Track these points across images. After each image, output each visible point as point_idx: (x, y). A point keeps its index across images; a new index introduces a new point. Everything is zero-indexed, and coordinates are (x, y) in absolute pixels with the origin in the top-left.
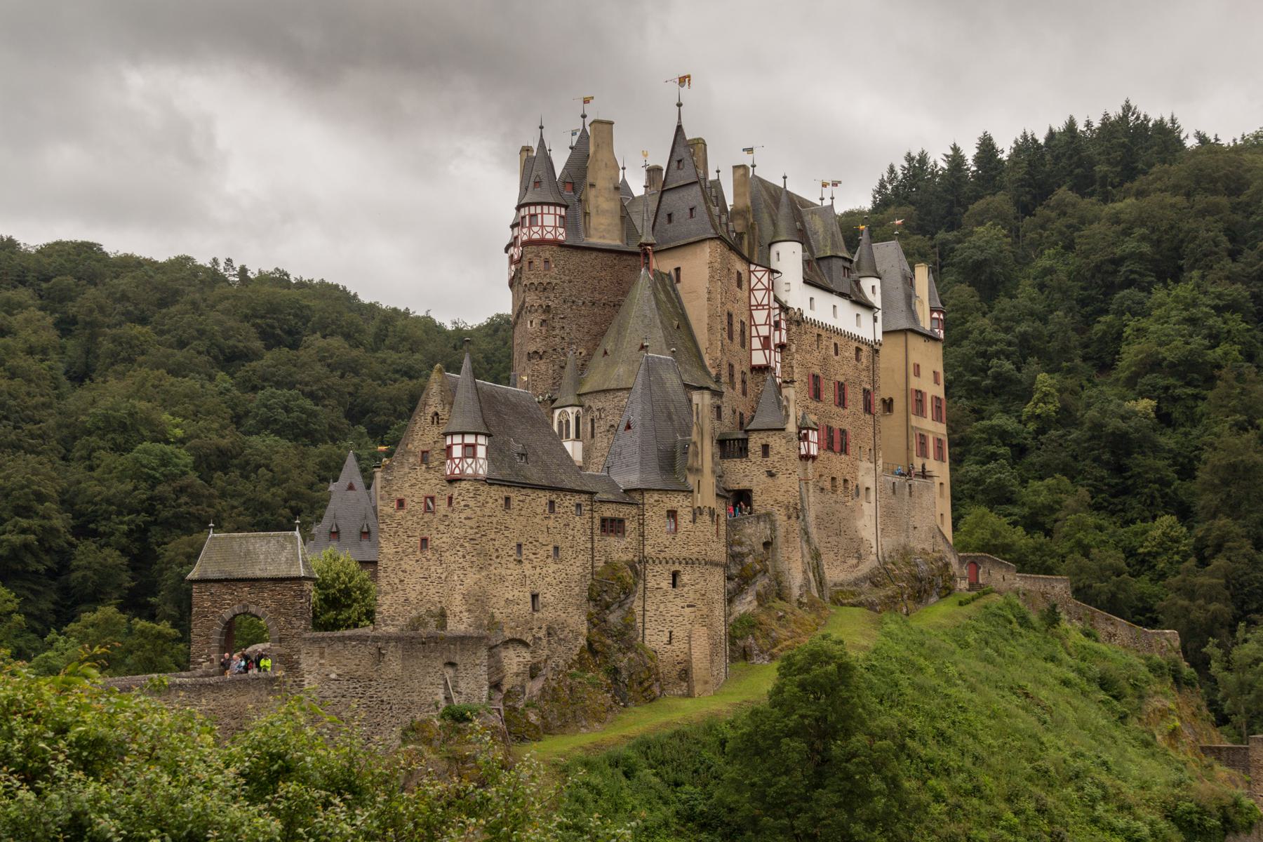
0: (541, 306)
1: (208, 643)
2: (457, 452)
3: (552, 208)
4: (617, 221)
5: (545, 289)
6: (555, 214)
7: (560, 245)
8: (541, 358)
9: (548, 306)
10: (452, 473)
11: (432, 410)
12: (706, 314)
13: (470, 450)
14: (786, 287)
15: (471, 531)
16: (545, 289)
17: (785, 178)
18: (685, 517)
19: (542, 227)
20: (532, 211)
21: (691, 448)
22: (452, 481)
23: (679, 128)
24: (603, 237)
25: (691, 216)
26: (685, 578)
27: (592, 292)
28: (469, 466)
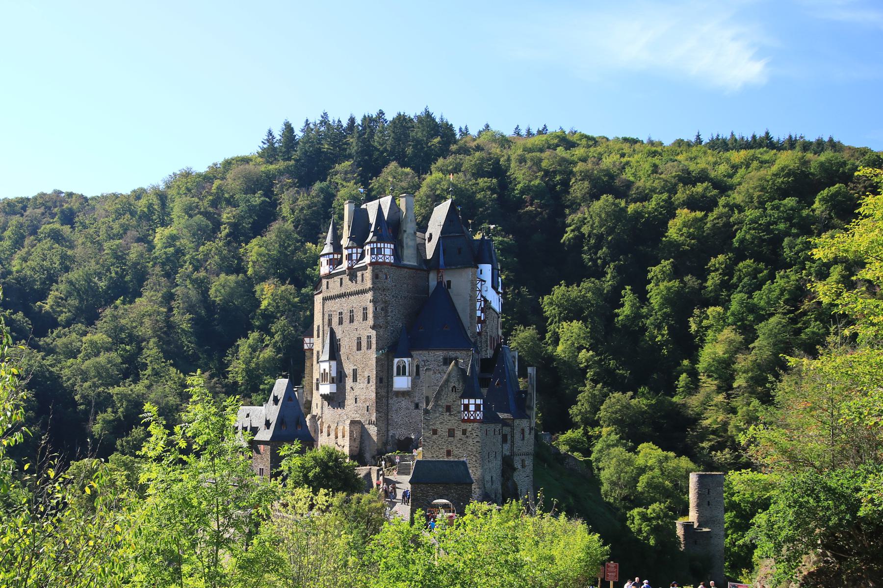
2: (472, 408)
5: (384, 290)
8: (381, 327)
10: (469, 418)
11: (453, 384)
12: (469, 308)
14: (485, 289)
15: (479, 448)
16: (384, 290)
18: (527, 431)
19: (384, 255)
20: (379, 246)
21: (529, 396)
22: (464, 421)
24: (409, 261)
25: (460, 253)
26: (526, 462)
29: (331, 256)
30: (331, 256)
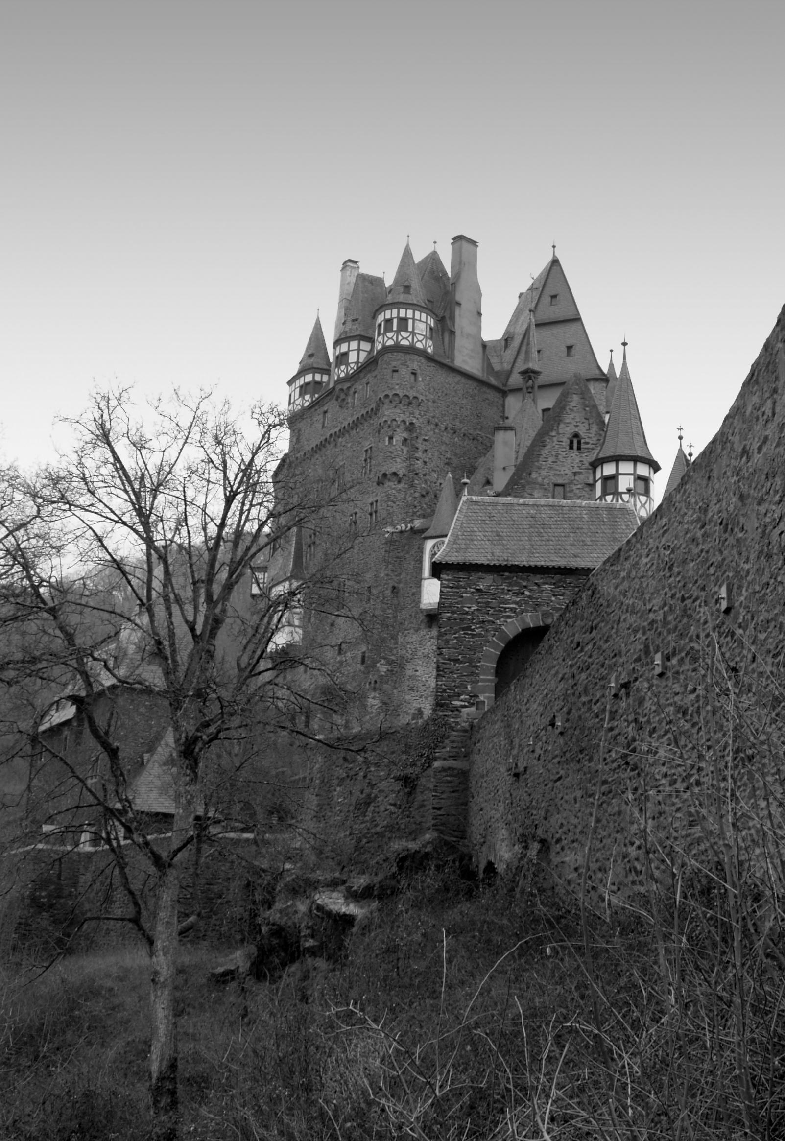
0: (404, 422)
1: (472, 674)
3: (424, 315)
4: (480, 349)
5: (410, 403)
6: (426, 322)
7: (429, 358)
8: (399, 482)
9: (411, 424)
13: (641, 484)
17: (611, 351)
19: (413, 333)
20: (402, 313)
23: (555, 262)
25: (568, 355)
27: (454, 419)
28: (643, 505)
29: (309, 378)
30: (309, 378)
